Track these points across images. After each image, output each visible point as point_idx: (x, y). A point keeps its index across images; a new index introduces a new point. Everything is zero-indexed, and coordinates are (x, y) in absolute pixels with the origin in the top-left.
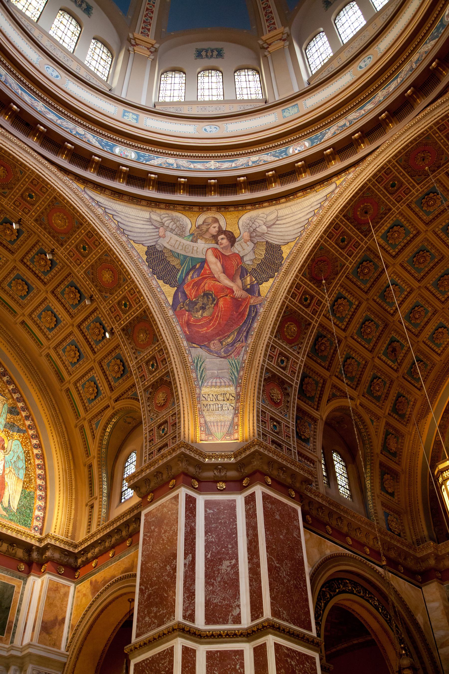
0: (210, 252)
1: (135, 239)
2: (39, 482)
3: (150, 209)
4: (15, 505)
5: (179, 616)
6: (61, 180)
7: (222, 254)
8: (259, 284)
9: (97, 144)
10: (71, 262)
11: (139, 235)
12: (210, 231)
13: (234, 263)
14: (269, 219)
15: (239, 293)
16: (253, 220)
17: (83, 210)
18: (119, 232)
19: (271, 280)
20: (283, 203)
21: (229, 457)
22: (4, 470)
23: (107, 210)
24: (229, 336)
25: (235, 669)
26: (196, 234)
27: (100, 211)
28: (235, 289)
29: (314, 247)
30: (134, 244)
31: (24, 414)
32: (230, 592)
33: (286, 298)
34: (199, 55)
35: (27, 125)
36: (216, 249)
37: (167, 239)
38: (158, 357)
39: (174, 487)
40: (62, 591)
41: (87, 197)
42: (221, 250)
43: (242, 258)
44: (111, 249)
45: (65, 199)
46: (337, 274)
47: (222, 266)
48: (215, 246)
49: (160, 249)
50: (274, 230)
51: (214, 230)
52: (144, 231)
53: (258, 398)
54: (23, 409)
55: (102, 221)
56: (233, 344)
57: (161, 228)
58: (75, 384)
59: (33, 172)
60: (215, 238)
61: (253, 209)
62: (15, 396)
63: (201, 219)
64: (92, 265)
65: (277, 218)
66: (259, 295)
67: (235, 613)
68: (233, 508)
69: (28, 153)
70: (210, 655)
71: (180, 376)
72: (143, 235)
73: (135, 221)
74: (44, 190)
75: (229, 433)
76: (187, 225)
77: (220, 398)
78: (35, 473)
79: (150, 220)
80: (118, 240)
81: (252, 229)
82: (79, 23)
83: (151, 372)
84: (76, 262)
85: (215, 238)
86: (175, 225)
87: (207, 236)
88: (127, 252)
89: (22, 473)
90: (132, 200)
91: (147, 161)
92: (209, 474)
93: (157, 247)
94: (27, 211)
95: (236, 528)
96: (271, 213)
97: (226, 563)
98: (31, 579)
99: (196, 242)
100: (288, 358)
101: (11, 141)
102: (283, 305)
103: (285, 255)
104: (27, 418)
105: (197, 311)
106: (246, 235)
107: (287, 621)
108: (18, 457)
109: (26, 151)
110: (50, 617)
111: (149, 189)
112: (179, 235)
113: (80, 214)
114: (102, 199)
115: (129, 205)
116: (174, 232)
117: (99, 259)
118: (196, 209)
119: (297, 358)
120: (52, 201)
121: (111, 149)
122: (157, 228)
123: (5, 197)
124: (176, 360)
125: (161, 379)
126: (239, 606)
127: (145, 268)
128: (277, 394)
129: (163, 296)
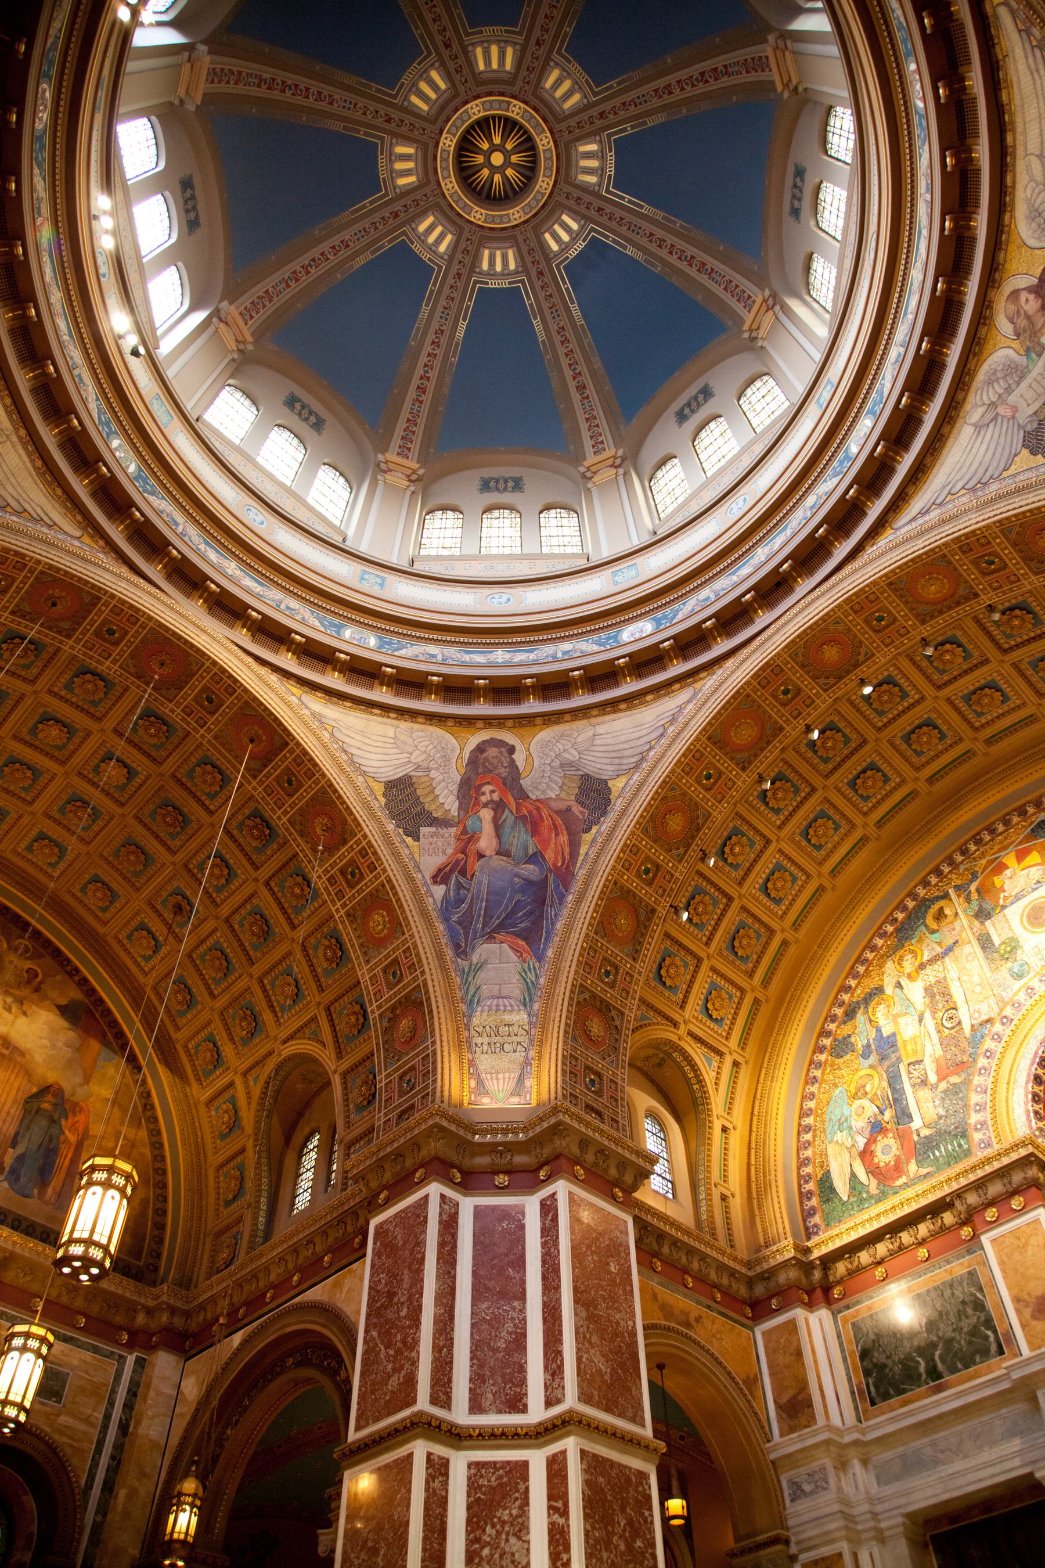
1: (1002, 466)
3: (960, 421)
6: (865, 565)
10: (1011, 590)
11: (997, 456)
12: (1030, 313)
17: (920, 546)
18: (980, 493)
20: (1014, 140)
23: (938, 501)
26: (1028, 343)
27: (935, 515)
30: (1010, 472)
34: (796, 212)
35: (778, 585)
37: (1022, 405)
41: (906, 529)
44: (999, 521)
45: (893, 571)
49: (1035, 425)
52: (992, 447)
55: (952, 518)
59: (839, 606)
61: (1012, 211)
63: (1003, 325)
64: (1024, 559)
69: (813, 601)
72: (1000, 449)
73: (971, 456)
74: (872, 597)
76: (1007, 357)
79: (979, 427)
80: (992, 501)
82: (715, 417)
84: (1012, 583)
86: (1001, 382)
88: (1019, 491)
90: (935, 449)
93: (1029, 428)
94: (902, 631)
109: (810, 604)
111: (925, 413)
112: (1022, 378)
113: (925, 553)
114: (918, 503)
115: (942, 457)
116: (1013, 386)
117: (1014, 545)
118: (983, 331)
120: (895, 590)
122: (995, 418)
123: (873, 655)
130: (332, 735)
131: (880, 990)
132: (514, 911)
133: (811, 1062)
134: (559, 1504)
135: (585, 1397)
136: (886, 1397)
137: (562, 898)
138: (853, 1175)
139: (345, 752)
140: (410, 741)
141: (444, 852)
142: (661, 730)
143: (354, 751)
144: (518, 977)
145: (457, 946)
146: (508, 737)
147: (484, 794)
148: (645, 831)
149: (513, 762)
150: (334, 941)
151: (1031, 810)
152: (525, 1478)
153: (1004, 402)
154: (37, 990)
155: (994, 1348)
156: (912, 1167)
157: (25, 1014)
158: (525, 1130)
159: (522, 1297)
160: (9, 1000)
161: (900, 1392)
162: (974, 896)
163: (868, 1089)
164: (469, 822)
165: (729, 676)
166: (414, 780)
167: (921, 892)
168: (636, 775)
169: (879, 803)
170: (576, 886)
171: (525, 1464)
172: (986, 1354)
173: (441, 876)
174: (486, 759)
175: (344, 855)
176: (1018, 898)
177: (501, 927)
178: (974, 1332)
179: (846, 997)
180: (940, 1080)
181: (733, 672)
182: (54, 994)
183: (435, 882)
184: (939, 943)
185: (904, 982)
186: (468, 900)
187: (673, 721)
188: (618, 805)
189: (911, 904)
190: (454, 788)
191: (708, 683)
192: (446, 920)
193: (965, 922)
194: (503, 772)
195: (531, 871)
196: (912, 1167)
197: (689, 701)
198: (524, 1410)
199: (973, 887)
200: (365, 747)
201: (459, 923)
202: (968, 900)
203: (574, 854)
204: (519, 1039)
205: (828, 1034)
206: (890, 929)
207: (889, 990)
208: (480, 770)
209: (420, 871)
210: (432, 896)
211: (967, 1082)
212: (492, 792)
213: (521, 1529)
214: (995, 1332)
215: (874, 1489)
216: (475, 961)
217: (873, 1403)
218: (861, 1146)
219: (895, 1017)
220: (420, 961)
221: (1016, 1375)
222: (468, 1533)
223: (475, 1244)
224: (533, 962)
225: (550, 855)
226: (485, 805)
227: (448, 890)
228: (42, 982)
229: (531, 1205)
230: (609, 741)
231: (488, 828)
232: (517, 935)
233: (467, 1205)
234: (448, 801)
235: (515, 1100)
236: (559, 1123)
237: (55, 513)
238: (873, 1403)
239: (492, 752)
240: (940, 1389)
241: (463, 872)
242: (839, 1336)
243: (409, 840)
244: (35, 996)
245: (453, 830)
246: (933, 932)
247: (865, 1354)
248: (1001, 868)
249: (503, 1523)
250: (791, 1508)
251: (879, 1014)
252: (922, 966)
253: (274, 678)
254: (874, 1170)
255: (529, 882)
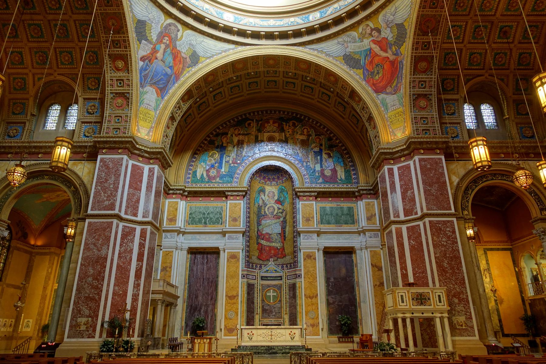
0: (371, 43)
1: (336, 55)
2: (350, 164)
3: (336, 38)
4: (343, 177)
5: (392, 218)
7: (378, 41)
8: (399, 48)
9: (302, 22)
11: (337, 53)
12: (367, 32)
13: (384, 43)
14: (392, 11)
15: (392, 58)
16: (385, 16)
19: (404, 44)
21: (403, 146)
22: (334, 166)
23: (319, 50)
24: (394, 82)
25: (417, 231)
28: (389, 56)
29: (417, 18)
30: (337, 58)
31: (334, 138)
32: (412, 203)
33: (412, 53)
36: (373, 40)
38: (365, 107)
39: (383, 166)
40: (371, 204)
42: (376, 39)
43: (387, 39)
46: (439, 22)
47: (380, 47)
48: (373, 38)
50: (397, 16)
51: (368, 31)
53: (411, 111)
54: (334, 136)
56: (396, 86)
57: (345, 44)
58: (349, 118)
60: (371, 34)
62: (328, 133)
63: (360, 30)
65: (396, 9)
66: (402, 54)
67: (415, 211)
68: (410, 167)
70: (408, 228)
71: (376, 113)
72: (338, 52)
73: (332, 47)
75: (404, 132)
77: (397, 115)
78: (347, 161)
79: (339, 43)
81: (386, 21)
83: (366, 113)
85: (371, 34)
87: (367, 36)
89: (342, 163)
91: (325, 14)
92: (397, 155)
93: (347, 53)
95: (412, 176)
96: (392, 7)
97: (409, 192)
98: (359, 202)
99: (363, 41)
100: (425, 82)
101: (268, 48)
102: (412, 58)
103: (406, 27)
104: (336, 139)
105: (376, 76)
106: (383, 25)
107: (436, 210)
108: (338, 158)
110: (369, 215)
112: (354, 42)
115: (327, 41)
119: (431, 78)
121: (308, 20)
122: (343, 44)
124: (372, 106)
125: (369, 116)
126: (416, 208)
127: (345, 67)
128: (423, 103)
129: (358, 77)
131: (227, 134)
132: (160, 81)
133: (202, 142)
134: (143, 239)
135: (152, 218)
136: (193, 224)
137: (174, 83)
138: (203, 174)
140: (151, 10)
141: (147, 51)
142: (221, 52)
143: (133, 3)
144: (155, 101)
145: (141, 84)
146: (179, 26)
147: (165, 39)
148: (203, 78)
149: (177, 35)
150: (95, 55)
151: (282, 113)
152: (135, 231)
153: (347, 43)
155: (220, 223)
156: (218, 179)
158: (150, 148)
159: (140, 190)
161: (196, 224)
162: (259, 125)
163: (214, 156)
164: (157, 46)
165: (246, 50)
166: (147, 23)
167: (248, 116)
168: (208, 60)
169: (251, 90)
170: (180, 82)
171: (135, 228)
172: (218, 223)
173: (143, 59)
174: (170, 29)
175: (117, 37)
176: (269, 132)
177: (155, 83)
178: (218, 218)
179: (218, 130)
180: (232, 163)
181: (247, 50)
183: (141, 60)
184: (246, 131)
185: (234, 135)
186: (148, 71)
187: (225, 51)
188: (200, 65)
189: (244, 117)
190: (157, 33)
191: (240, 48)
192: (141, 74)
193: (254, 130)
194: (173, 36)
195: (169, 71)
196: (218, 179)
197: (232, 49)
198: (137, 216)
199: (260, 123)
200: (136, 4)
202: (257, 124)
203: (182, 72)
204: (151, 120)
205: (209, 137)
206: (236, 120)
207: (229, 135)
208: (167, 31)
209: (138, 54)
211: (238, 167)
212: (167, 40)
213: (132, 241)
214: (222, 220)
215: (183, 241)
216: (145, 90)
217: (189, 224)
218: (207, 169)
219: (228, 143)
220: (132, 86)
221: (224, 230)
222: (121, 240)
223: (131, 174)
224: (160, 98)
225: (176, 68)
226: (164, 43)
227: (144, 64)
229: (146, 168)
230: (206, 45)
231: (161, 51)
232: (158, 87)
233: (131, 162)
234: (154, 36)
235: (146, 137)
236: (162, 152)
238: (189, 224)
239: (173, 28)
240: (205, 226)
241: (150, 61)
242: (186, 208)
245: (152, 46)
246: (246, 127)
247: (191, 214)
248: (268, 122)
249: (129, 240)
250: (163, 240)
251: (224, 140)
252: (239, 134)
254: (208, 175)
255: (166, 74)
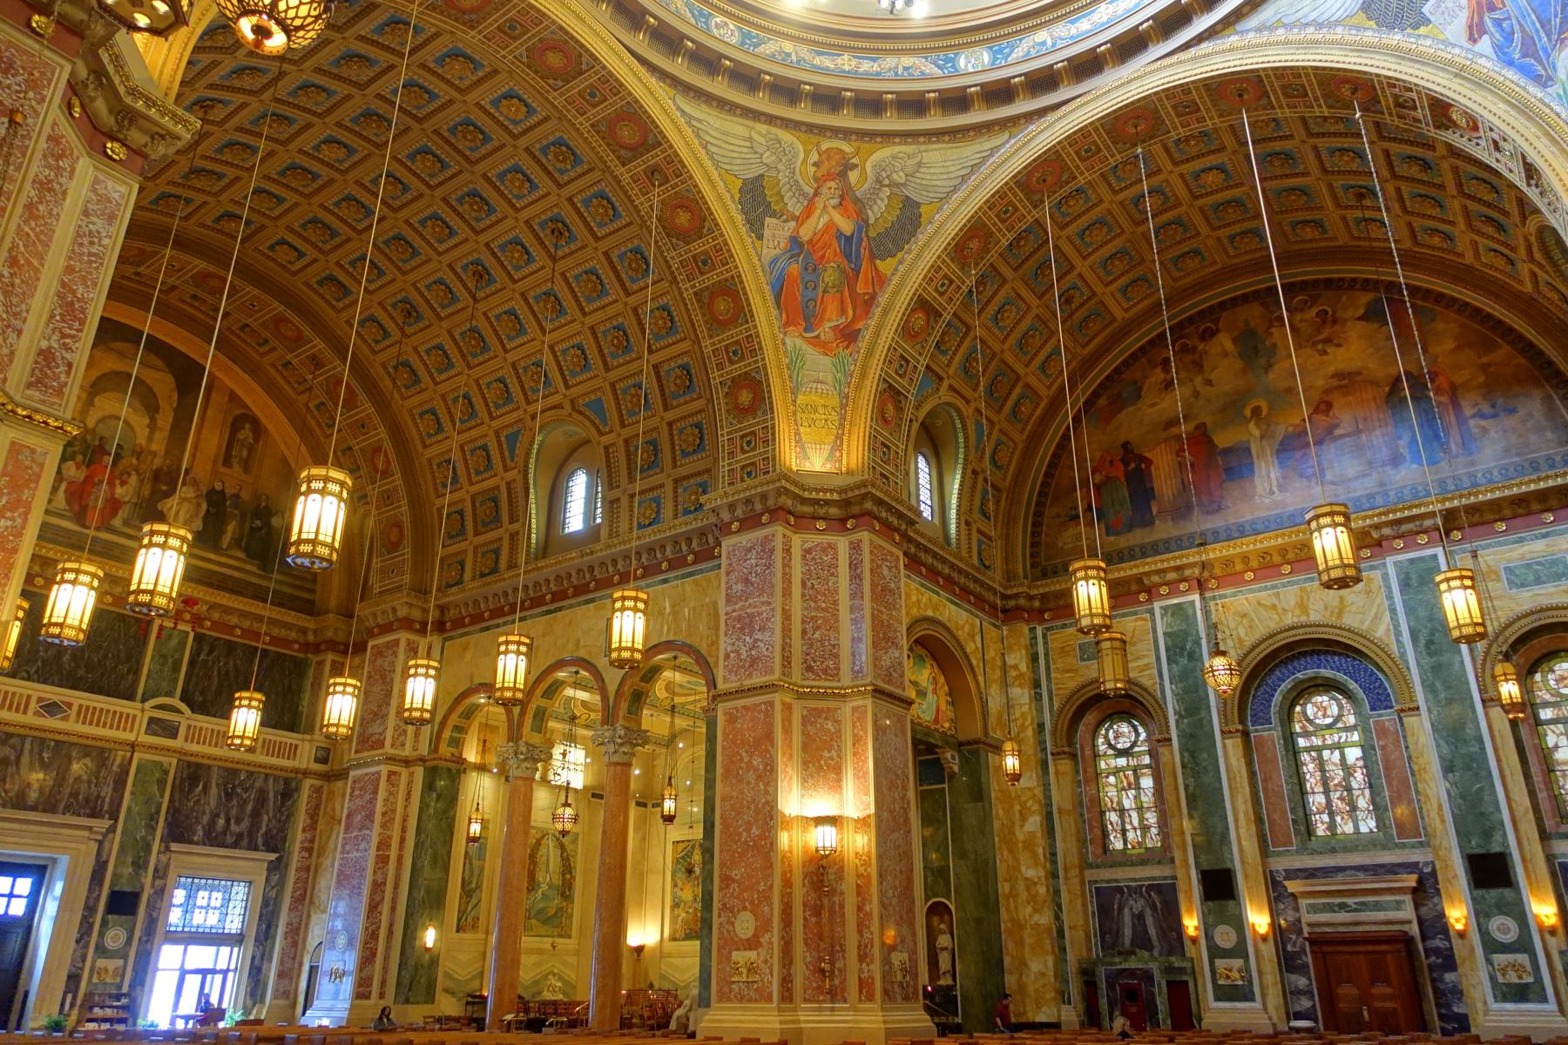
130: (1285, 26)
139: (1307, 25)
141: (1460, 7)
143: (1313, 16)
154: (1335, 322)
157: (1339, 345)
160: (1320, 346)
182: (1350, 313)
201: (1525, 55)
209: (1454, 45)
210: (1482, 56)
228: (1334, 313)
237: (986, 144)
243: (1422, 30)
244: (1337, 327)
253: (1206, 47)
